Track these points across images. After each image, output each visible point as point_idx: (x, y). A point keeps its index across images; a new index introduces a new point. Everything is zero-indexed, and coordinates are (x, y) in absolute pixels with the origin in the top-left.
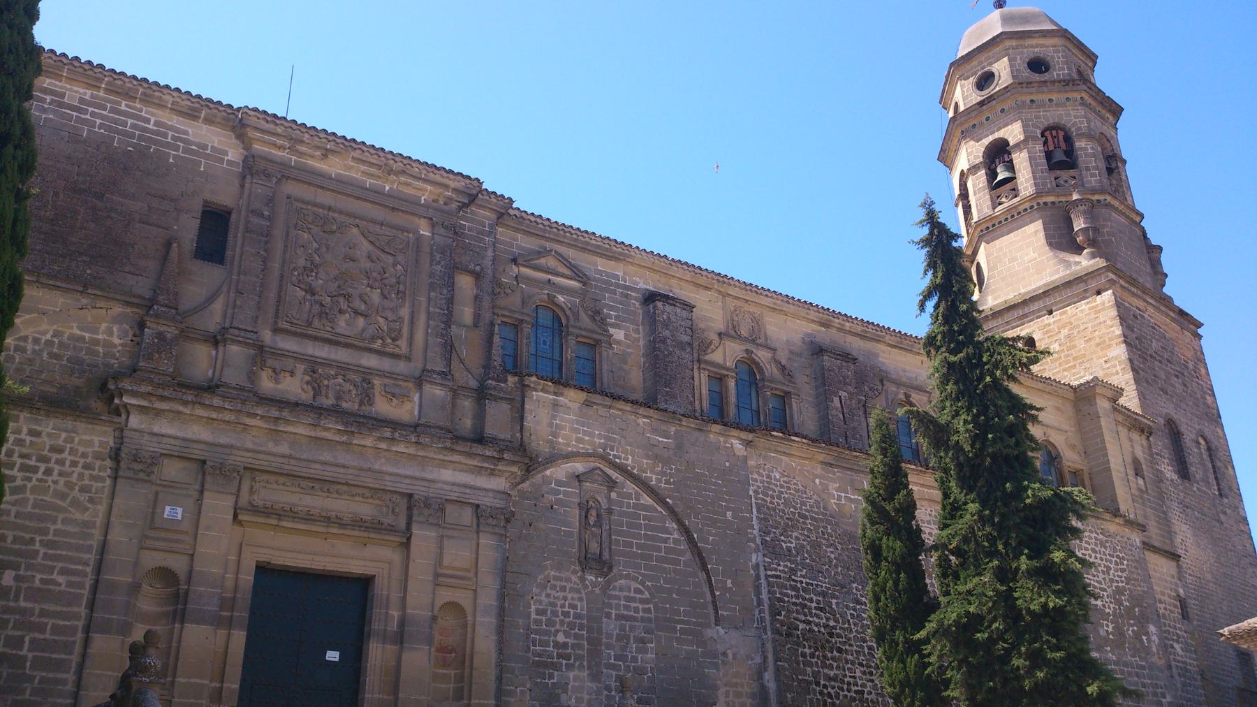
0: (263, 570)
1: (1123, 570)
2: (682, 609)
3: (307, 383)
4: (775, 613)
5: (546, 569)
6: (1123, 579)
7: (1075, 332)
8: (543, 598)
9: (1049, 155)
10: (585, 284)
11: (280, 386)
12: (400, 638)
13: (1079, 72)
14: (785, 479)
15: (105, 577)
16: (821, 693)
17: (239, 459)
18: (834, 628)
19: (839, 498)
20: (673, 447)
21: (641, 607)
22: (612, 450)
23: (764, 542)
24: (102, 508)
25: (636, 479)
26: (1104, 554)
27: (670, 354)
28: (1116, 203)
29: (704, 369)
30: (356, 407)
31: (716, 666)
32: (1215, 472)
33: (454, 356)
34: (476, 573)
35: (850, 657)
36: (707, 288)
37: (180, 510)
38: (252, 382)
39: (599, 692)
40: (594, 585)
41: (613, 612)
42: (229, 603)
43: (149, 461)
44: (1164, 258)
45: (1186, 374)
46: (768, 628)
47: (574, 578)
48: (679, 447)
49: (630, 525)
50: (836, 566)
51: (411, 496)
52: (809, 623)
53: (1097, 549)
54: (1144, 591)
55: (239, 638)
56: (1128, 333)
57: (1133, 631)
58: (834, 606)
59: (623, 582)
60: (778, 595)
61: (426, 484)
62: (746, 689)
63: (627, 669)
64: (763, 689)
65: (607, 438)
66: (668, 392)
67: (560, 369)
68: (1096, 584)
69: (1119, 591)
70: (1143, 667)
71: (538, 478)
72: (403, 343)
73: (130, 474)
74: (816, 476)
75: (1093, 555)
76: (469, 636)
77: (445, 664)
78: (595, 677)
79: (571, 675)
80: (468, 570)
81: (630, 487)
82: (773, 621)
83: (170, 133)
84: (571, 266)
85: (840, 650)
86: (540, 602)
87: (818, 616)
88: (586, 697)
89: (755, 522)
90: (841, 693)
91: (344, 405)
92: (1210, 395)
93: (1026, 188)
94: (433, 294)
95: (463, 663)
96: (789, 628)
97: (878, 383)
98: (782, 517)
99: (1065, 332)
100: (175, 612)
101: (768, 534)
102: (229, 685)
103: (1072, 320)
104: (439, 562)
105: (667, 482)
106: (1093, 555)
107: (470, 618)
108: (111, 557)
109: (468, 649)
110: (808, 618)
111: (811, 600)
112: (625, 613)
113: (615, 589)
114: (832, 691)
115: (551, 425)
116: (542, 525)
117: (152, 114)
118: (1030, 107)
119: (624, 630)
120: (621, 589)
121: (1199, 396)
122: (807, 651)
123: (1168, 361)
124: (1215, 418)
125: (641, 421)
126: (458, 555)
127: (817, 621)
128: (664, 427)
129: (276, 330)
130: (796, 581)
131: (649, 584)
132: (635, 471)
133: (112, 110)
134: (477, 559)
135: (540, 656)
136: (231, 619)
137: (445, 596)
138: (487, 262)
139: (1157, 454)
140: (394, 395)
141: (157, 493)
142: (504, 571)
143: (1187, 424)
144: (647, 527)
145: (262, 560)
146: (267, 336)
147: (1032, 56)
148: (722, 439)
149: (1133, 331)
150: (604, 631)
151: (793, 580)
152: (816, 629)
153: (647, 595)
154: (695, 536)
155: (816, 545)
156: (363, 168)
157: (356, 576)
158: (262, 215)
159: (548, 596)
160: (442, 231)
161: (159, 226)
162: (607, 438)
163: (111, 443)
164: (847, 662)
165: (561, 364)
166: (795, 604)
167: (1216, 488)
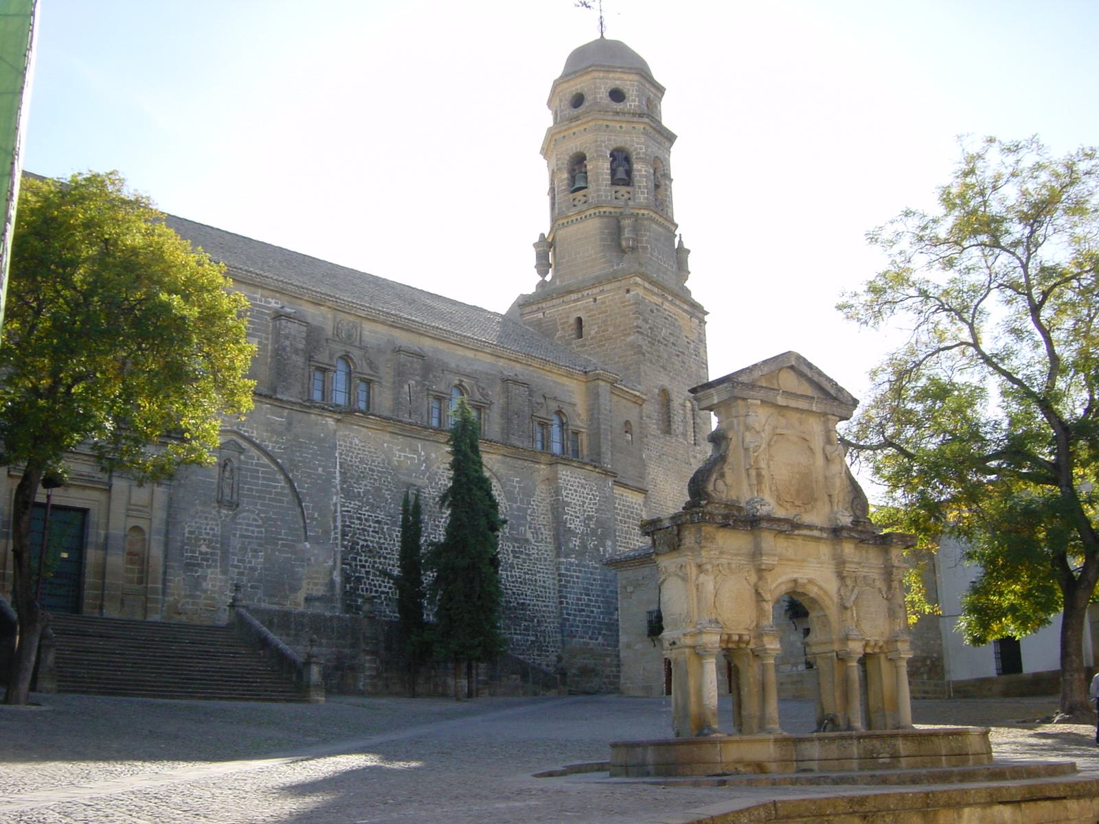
1: (595, 504)
2: (283, 531)
4: (344, 534)
7: (609, 319)
9: (613, 172)
18: (384, 543)
19: (400, 457)
21: (256, 530)
23: (342, 489)
25: (258, 447)
27: (289, 358)
28: (657, 217)
31: (303, 566)
32: (694, 427)
34: (152, 509)
35: (391, 562)
36: (322, 305)
39: (226, 581)
40: (227, 516)
41: (238, 533)
48: (290, 424)
50: (390, 504)
52: (366, 541)
57: (594, 544)
58: (385, 530)
59: (245, 514)
60: (348, 523)
63: (245, 568)
66: (284, 386)
69: (589, 518)
70: (596, 568)
75: (575, 494)
76: (147, 547)
77: (132, 562)
78: (224, 572)
79: (209, 571)
80: (146, 507)
81: (254, 452)
82: (343, 539)
85: (385, 558)
86: (191, 526)
87: (373, 537)
88: (218, 584)
89: (338, 474)
97: (440, 372)
98: (356, 471)
104: (129, 502)
105: (280, 448)
106: (575, 494)
107: (147, 537)
109: (146, 555)
110: (367, 538)
111: (370, 526)
112: (246, 533)
113: (239, 518)
116: (194, 478)
118: (605, 131)
121: (694, 369)
122: (363, 558)
123: (673, 344)
126: (141, 495)
127: (372, 539)
128: (280, 410)
131: (262, 515)
132: (258, 442)
134: (152, 500)
137: (133, 522)
143: (678, 393)
144: (264, 478)
147: (614, 87)
148: (320, 418)
149: (647, 323)
152: (371, 544)
153: (260, 522)
154: (296, 484)
155: (378, 489)
164: (389, 565)
166: (358, 529)
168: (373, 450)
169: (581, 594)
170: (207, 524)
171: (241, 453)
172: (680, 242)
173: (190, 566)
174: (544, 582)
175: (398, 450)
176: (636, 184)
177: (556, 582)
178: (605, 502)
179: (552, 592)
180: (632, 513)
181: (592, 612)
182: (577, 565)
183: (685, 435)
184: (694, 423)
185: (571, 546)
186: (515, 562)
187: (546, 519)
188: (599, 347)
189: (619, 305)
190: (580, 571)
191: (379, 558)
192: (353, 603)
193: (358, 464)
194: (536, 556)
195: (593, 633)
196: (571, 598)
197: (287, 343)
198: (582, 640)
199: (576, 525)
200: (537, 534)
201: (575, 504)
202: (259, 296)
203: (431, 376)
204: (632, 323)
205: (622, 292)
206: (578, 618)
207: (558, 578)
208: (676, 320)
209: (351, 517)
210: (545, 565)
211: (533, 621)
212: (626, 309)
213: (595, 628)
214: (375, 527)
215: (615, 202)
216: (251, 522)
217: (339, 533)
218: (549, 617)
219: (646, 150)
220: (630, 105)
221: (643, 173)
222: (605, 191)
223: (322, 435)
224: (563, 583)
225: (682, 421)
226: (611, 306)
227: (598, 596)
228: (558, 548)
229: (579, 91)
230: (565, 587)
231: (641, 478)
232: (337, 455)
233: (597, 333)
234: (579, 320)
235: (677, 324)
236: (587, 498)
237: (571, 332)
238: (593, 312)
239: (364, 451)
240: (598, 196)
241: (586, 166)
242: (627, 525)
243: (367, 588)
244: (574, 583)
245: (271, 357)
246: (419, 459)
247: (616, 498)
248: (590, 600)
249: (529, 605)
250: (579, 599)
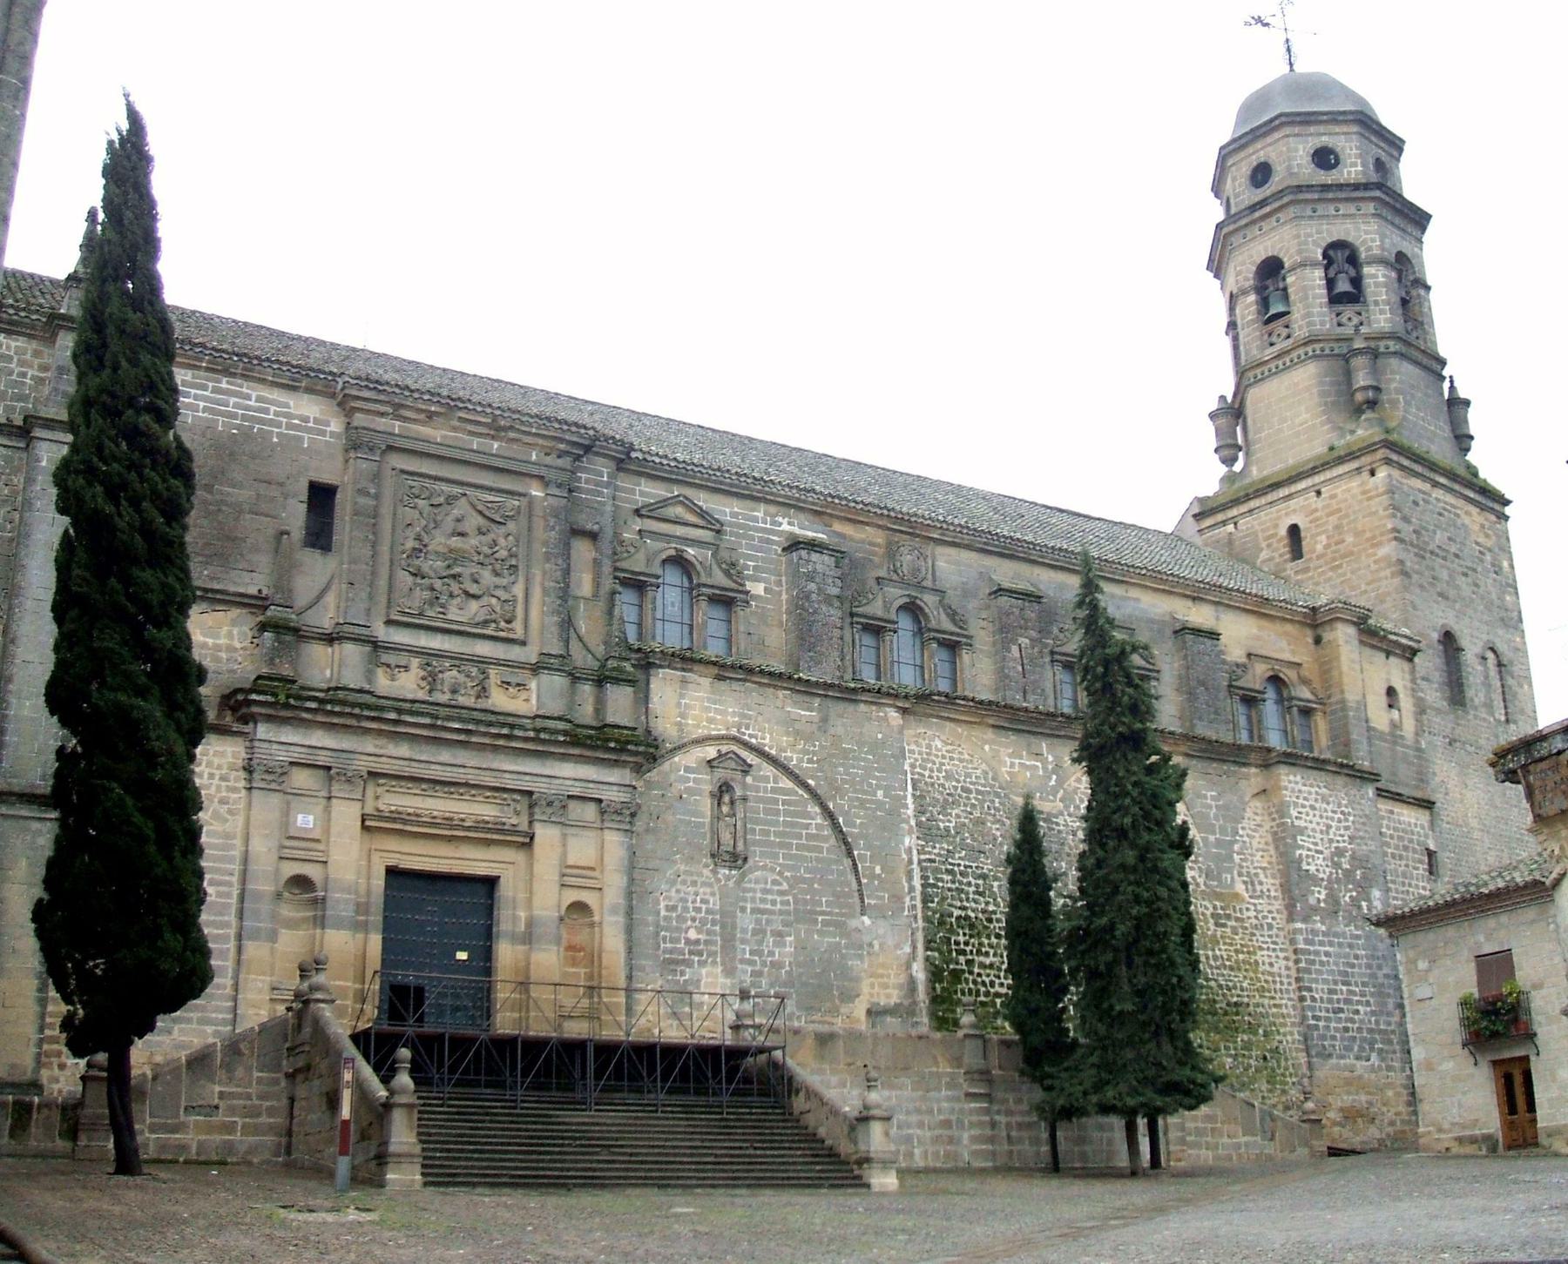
0: (392, 873)
1: (1347, 828)
3: (423, 679)
4: (926, 900)
5: (675, 862)
6: (1346, 838)
7: (1345, 522)
8: (673, 893)
9: (1330, 284)
10: (718, 532)
11: (396, 683)
12: (528, 937)
13: (1379, 165)
14: (950, 748)
15: (250, 886)
16: (975, 982)
17: (363, 764)
18: (994, 912)
19: (1012, 765)
20: (816, 720)
22: (747, 728)
23: (919, 824)
24: (241, 820)
25: (774, 761)
26: (1326, 811)
29: (857, 623)
30: (473, 700)
31: (861, 957)
32: (1503, 693)
33: (573, 635)
37: (311, 818)
38: (370, 681)
40: (728, 878)
41: (749, 906)
42: (362, 908)
43: (279, 770)
44: (1473, 416)
45: (1479, 569)
46: (920, 915)
47: (706, 872)
48: (825, 720)
49: (766, 811)
50: (1001, 844)
51: (530, 793)
52: (964, 908)
53: (1317, 805)
54: (1371, 851)
55: (375, 942)
56: (1402, 525)
58: (995, 889)
60: (931, 881)
61: (547, 780)
62: (893, 980)
63: (764, 964)
64: (912, 981)
65: (743, 716)
67: (691, 633)
68: (1312, 846)
69: (1340, 852)
70: (1358, 937)
71: (666, 766)
72: (518, 625)
73: (262, 785)
74: (986, 742)
75: (1311, 813)
77: (574, 965)
79: (704, 971)
80: (592, 869)
81: (768, 770)
82: (925, 907)
83: (273, 408)
84: (702, 514)
87: (975, 901)
89: (910, 800)
90: (997, 981)
91: (462, 700)
92: (1510, 594)
93: (1300, 328)
94: (547, 566)
95: (593, 962)
96: (942, 916)
99: (1333, 519)
100: (315, 917)
101: (923, 813)
103: (1343, 506)
105: (810, 761)
108: (252, 867)
109: (596, 945)
110: (965, 904)
111: (969, 884)
112: (762, 906)
113: (750, 881)
114: (987, 980)
115: (679, 704)
116: (670, 818)
117: (253, 389)
119: (760, 924)
120: (757, 882)
121: (1494, 596)
122: (961, 939)
123: (1457, 556)
124: (1512, 621)
125: (781, 693)
126: (582, 849)
127: (973, 905)
128: (807, 698)
129: (389, 622)
130: (953, 865)
131: (787, 874)
132: (773, 752)
133: (216, 390)
135: (671, 951)
136: (366, 922)
137: (572, 896)
138: (606, 520)
139: (1423, 679)
140: (508, 683)
141: (288, 803)
142: (632, 867)
144: (787, 813)
146: (381, 632)
147: (1319, 146)
150: (739, 925)
151: (951, 864)
152: (973, 915)
153: (785, 886)
154: (841, 820)
155: (980, 822)
156: (470, 427)
158: (368, 494)
159: (678, 891)
160: (556, 491)
161: (267, 516)
162: (743, 716)
163: (244, 755)
165: (691, 626)
167: (1503, 712)
168: (966, 757)
169: (1335, 983)
170: (697, 894)
171: (745, 772)
172: (1452, 387)
173: (672, 964)
174: (1271, 965)
175: (1010, 756)
176: (1370, 299)
177: (1291, 964)
178: (1364, 824)
179: (1285, 980)
180: (1411, 841)
181: (1357, 1012)
182: (1325, 934)
183: (1489, 706)
184: (1503, 686)
185: (1312, 901)
186: (1219, 934)
187: (1267, 859)
188: (1333, 569)
189: (1360, 497)
190: (1331, 944)
191: (988, 937)
192: (951, 1016)
193: (942, 781)
194: (1254, 921)
195: (1361, 1049)
196: (1320, 990)
197: (812, 586)
198: (1342, 1062)
199: (1317, 865)
200: (1253, 883)
201: (1314, 830)
202: (760, 515)
203: (1055, 630)
204: (1385, 525)
205: (1366, 475)
206: (1333, 1025)
207: (1293, 957)
208: (1458, 516)
209: (937, 870)
210: (1270, 936)
211: (1256, 1033)
212: (1372, 503)
213: (1364, 1040)
214: (977, 886)
215: (1339, 330)
216: (769, 887)
217: (919, 898)
218: (1284, 1025)
219: (1381, 241)
220: (1349, 173)
221: (1381, 279)
222: (1321, 314)
223: (880, 736)
224: (1303, 965)
225: (1483, 684)
226: (1346, 500)
227: (1364, 984)
228: (1290, 908)
229: (1262, 160)
230: (1308, 971)
231: (1422, 780)
232: (907, 767)
233: (1327, 546)
234: (1294, 530)
235: (1459, 522)
236: (1332, 819)
237: (1283, 548)
238: (1318, 514)
239: (952, 759)
240: (1310, 324)
241: (1284, 279)
242: (1404, 862)
243: (970, 989)
244: (1322, 963)
245: (789, 612)
246: (1045, 768)
247: (1383, 818)
248: (1351, 992)
249: (1248, 1005)
250: (1331, 992)
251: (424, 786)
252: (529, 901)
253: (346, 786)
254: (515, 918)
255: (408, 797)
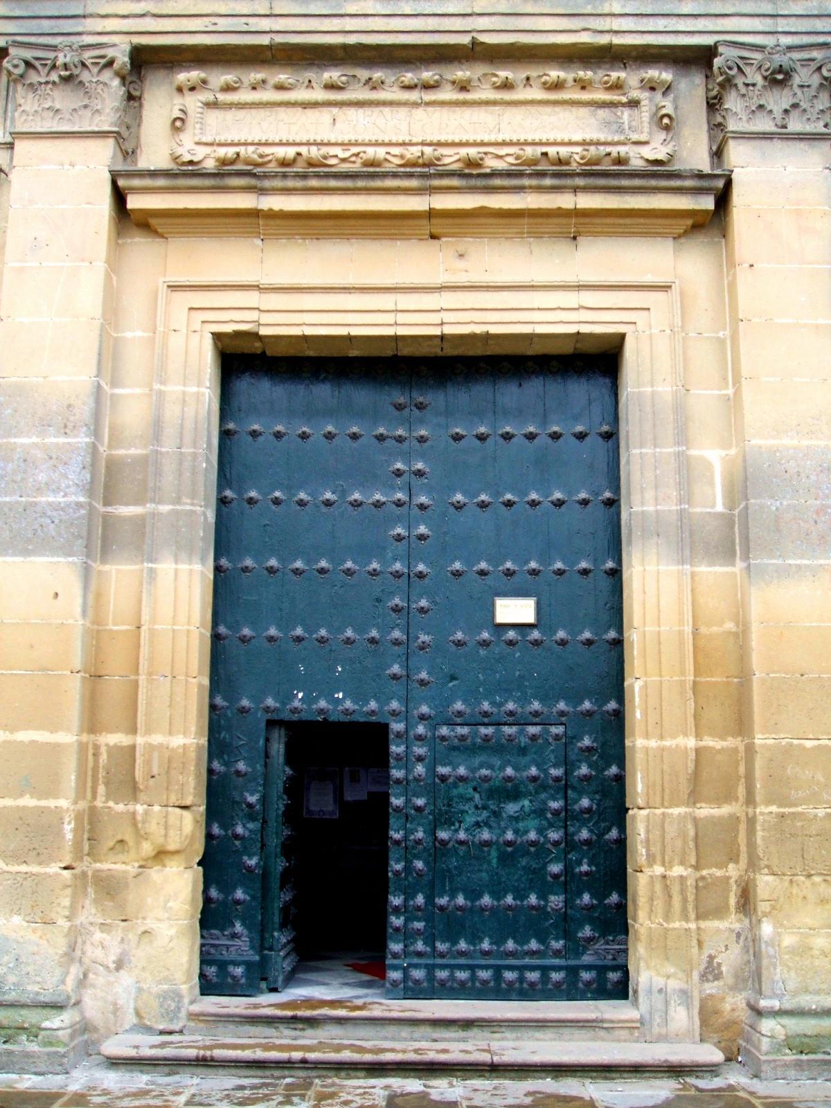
102: (157, 739)
145: (228, 328)
157: (568, 349)
251: (333, 75)
252: (733, 405)
253: (62, 99)
254: (686, 473)
255: (282, 113)
